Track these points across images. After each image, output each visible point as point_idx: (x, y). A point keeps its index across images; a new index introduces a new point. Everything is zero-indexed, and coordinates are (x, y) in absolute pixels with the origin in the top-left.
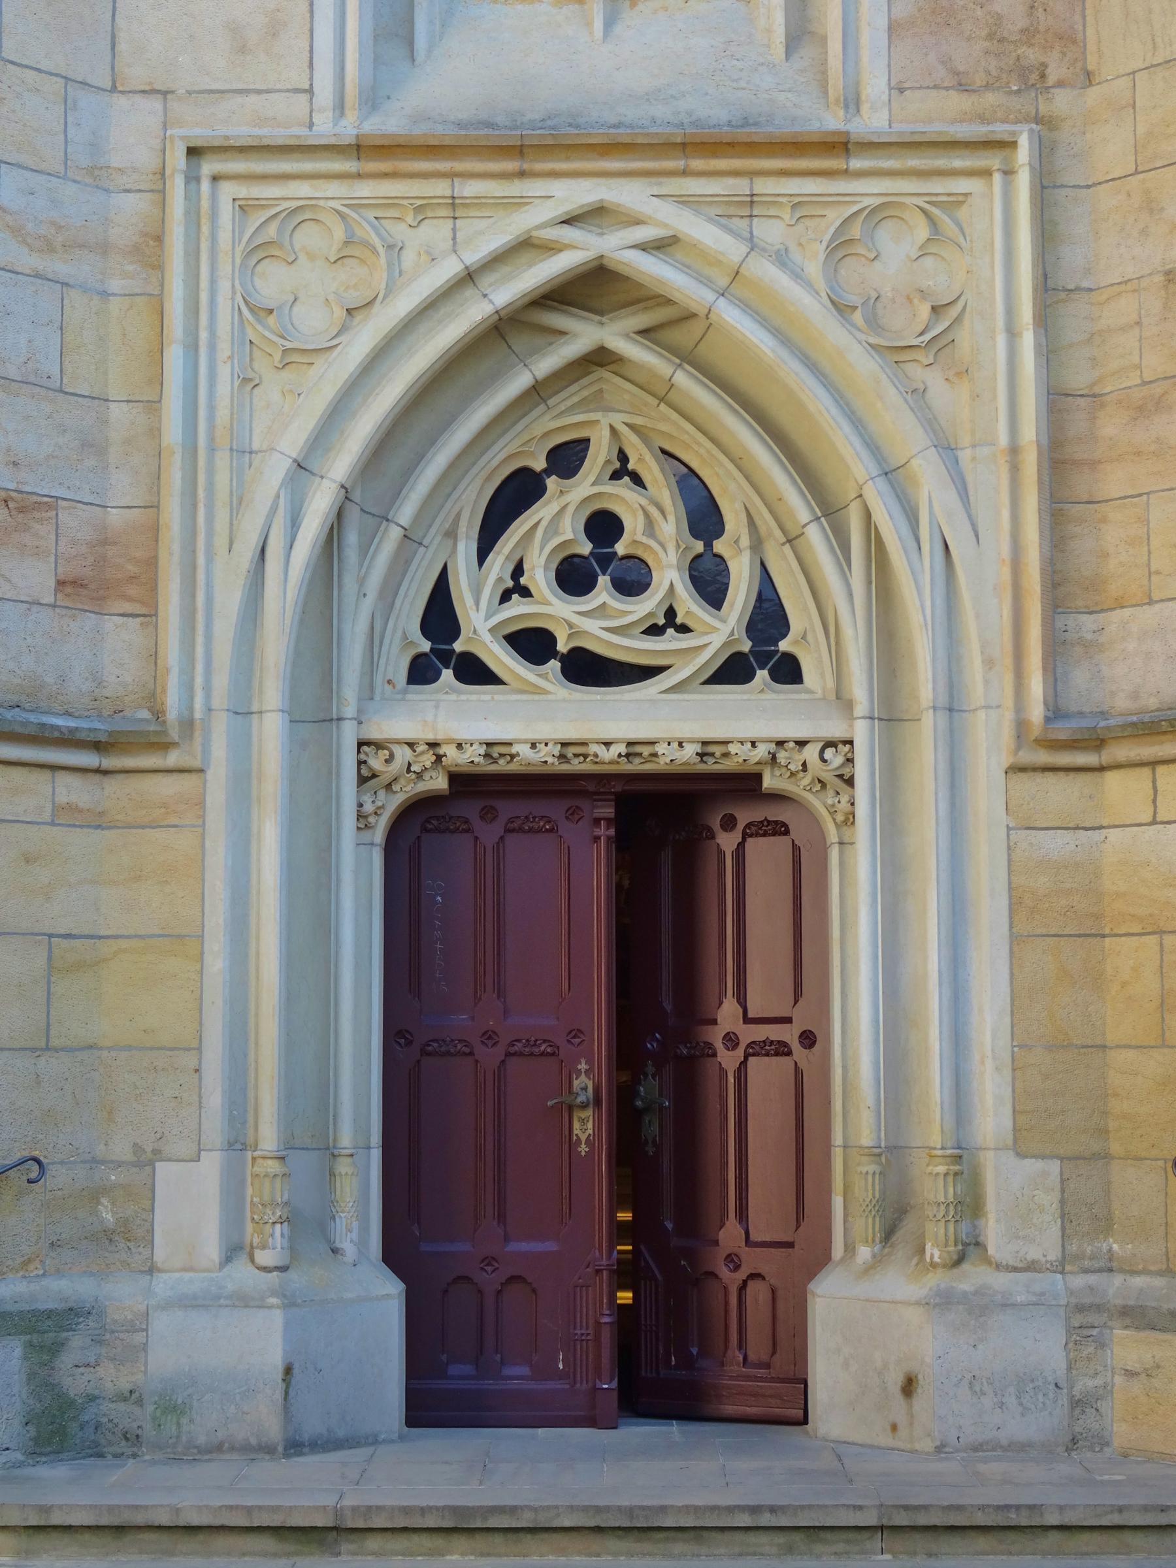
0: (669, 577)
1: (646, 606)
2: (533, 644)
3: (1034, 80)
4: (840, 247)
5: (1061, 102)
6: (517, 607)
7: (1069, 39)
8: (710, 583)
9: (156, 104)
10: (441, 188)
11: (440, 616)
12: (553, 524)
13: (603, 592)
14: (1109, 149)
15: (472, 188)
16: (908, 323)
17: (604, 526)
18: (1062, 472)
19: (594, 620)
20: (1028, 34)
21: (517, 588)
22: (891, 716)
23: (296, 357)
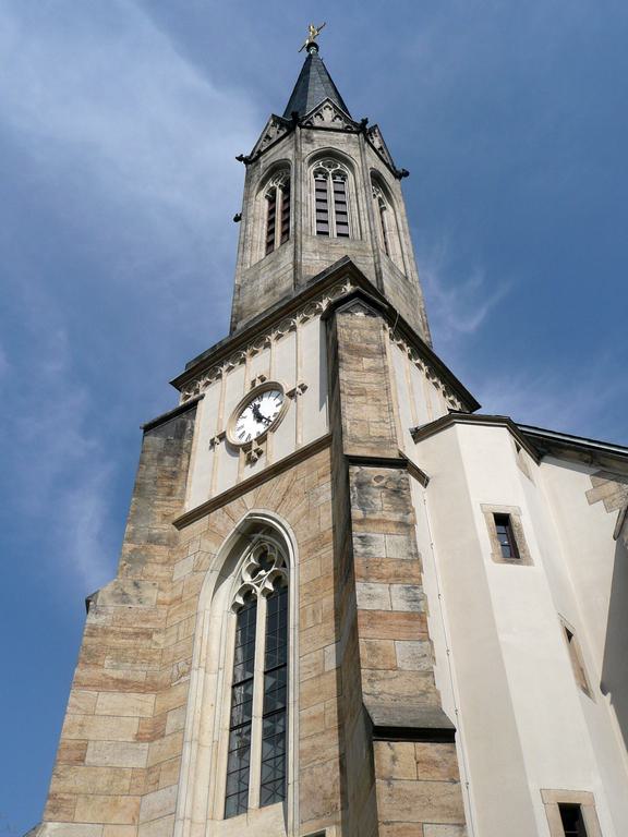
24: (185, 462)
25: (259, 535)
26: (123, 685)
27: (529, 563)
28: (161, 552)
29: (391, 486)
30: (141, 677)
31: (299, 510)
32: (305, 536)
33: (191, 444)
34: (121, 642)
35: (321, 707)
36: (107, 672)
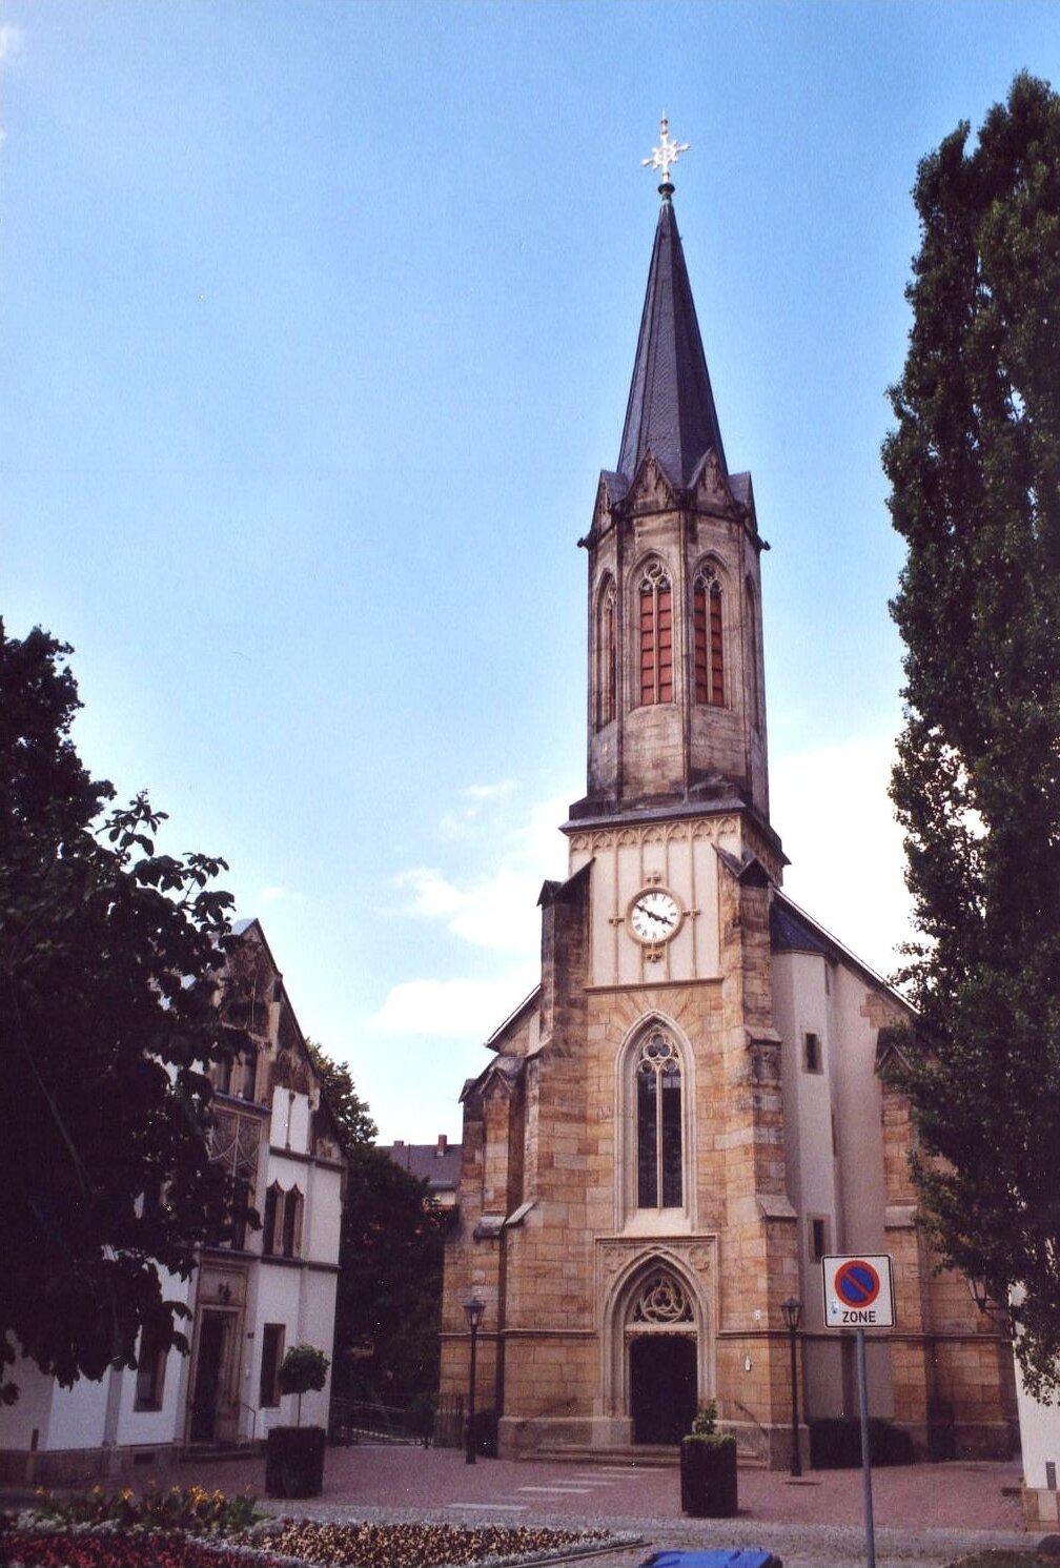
2: (652, 1314)
4: (691, 1254)
5: (724, 1229)
6: (651, 1308)
7: (725, 1218)
11: (639, 1310)
12: (655, 1295)
14: (728, 1237)
17: (663, 1294)
18: (722, 1292)
19: (662, 1310)
22: (701, 1327)
23: (614, 1272)
25: (657, 1026)
26: (567, 1117)
28: (577, 1014)
31: (695, 1028)
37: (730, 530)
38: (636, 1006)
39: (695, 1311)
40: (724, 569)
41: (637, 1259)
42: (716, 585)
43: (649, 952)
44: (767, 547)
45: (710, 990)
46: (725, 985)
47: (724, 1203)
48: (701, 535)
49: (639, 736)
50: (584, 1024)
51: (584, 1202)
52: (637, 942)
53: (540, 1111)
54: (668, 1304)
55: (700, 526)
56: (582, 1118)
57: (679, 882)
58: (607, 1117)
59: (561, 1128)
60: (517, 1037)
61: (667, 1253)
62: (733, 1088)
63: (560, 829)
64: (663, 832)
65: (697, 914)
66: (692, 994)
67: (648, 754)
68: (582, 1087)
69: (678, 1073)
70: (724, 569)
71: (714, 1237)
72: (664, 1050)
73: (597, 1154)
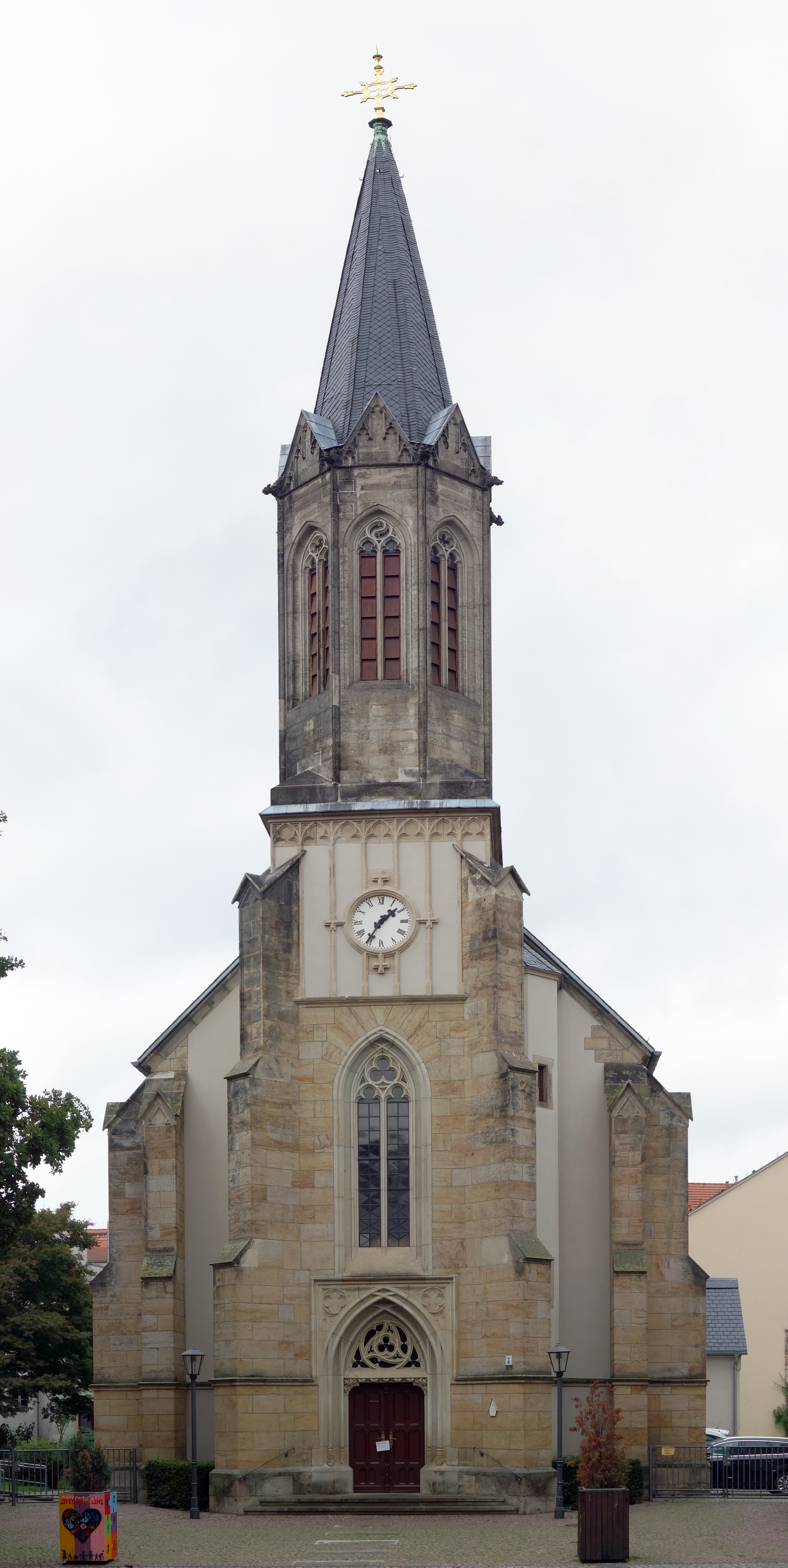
0: (398, 1349)
1: (393, 1354)
2: (374, 1360)
3: (457, 1266)
6: (371, 1354)
8: (404, 1349)
9: (308, 1272)
10: (357, 1286)
11: (358, 1355)
12: (377, 1339)
13: (386, 1351)
15: (361, 1286)
16: (435, 1309)
17: (386, 1339)
18: (460, 1335)
20: (456, 1258)
21: (371, 1351)
24: (295, 933)
26: (280, 1145)
27: (551, 1108)
29: (527, 1090)
30: (289, 1139)
32: (437, 1076)
33: (298, 912)
34: (275, 1111)
35: (449, 1207)
36: (270, 1134)
37: (474, 497)
38: (360, 1023)
39: (424, 1357)
40: (465, 538)
41: (362, 1301)
42: (452, 556)
43: (374, 963)
44: (499, 522)
45: (451, 1010)
46: (468, 1006)
47: (462, 1244)
48: (441, 497)
49: (363, 714)
50: (295, 1041)
51: (298, 1239)
52: (359, 949)
53: (252, 1138)
54: (391, 1348)
55: (440, 487)
56: (296, 1148)
57: (412, 885)
58: (325, 1146)
59: (274, 1157)
60: (172, 1055)
61: (394, 1295)
62: (478, 1119)
63: (261, 815)
64: (394, 827)
65: (435, 923)
66: (427, 1013)
67: (373, 736)
68: (295, 1113)
69: (406, 1100)
70: (465, 538)
71: (452, 1279)
72: (391, 1073)
73: (313, 1187)
